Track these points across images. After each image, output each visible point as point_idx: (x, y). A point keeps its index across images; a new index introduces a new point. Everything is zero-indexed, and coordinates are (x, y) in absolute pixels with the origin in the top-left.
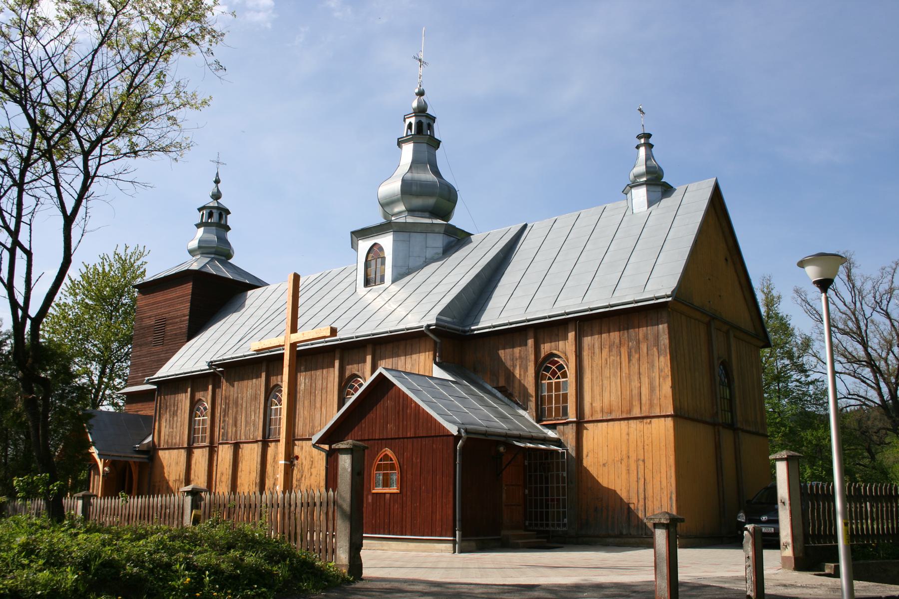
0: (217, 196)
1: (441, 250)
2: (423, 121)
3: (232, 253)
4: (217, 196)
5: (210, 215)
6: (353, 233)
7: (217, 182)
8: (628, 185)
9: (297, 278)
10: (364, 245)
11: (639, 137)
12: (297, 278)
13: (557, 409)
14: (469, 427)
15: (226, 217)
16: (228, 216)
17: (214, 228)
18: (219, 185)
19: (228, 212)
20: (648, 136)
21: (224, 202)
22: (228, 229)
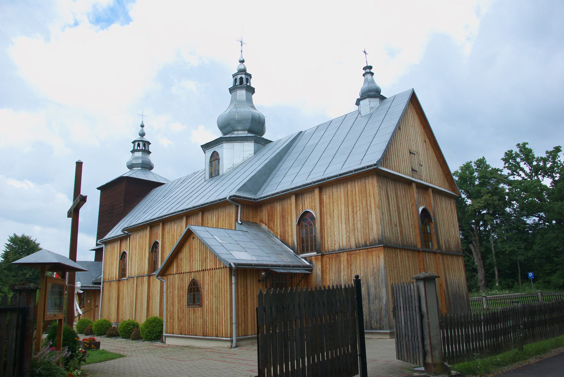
0: (142, 135)
1: (253, 152)
2: (243, 77)
3: (153, 166)
4: (142, 135)
5: (139, 145)
6: (202, 146)
7: (142, 126)
8: (357, 99)
9: (79, 165)
10: (209, 152)
11: (364, 69)
12: (79, 165)
13: (312, 245)
14: (237, 262)
15: (148, 146)
16: (150, 146)
17: (141, 152)
18: (143, 128)
19: (149, 143)
20: (370, 68)
21: (146, 138)
22: (149, 153)
